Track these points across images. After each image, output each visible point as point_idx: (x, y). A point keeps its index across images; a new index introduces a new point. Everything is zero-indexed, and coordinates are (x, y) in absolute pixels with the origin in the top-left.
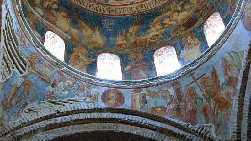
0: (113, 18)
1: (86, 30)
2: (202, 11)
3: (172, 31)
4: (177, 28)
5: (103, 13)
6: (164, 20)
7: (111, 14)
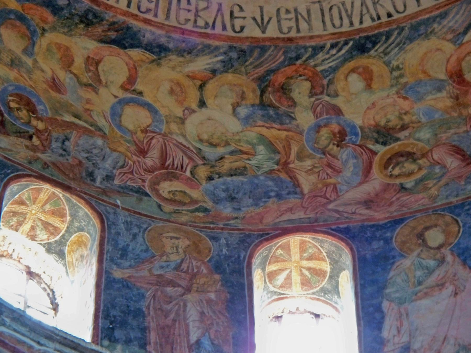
2: (41, 126)
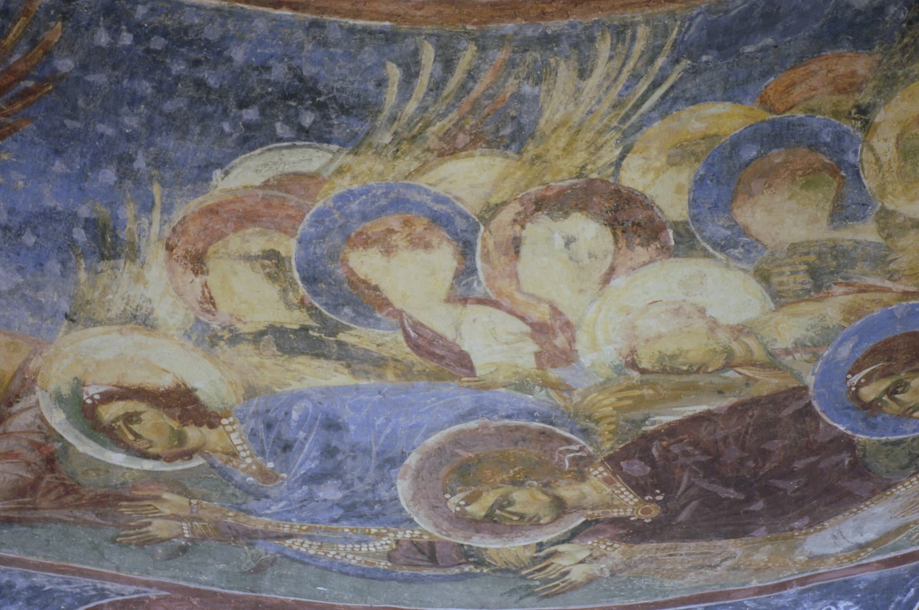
3: (440, 450)
4: (511, 454)
6: (366, 242)
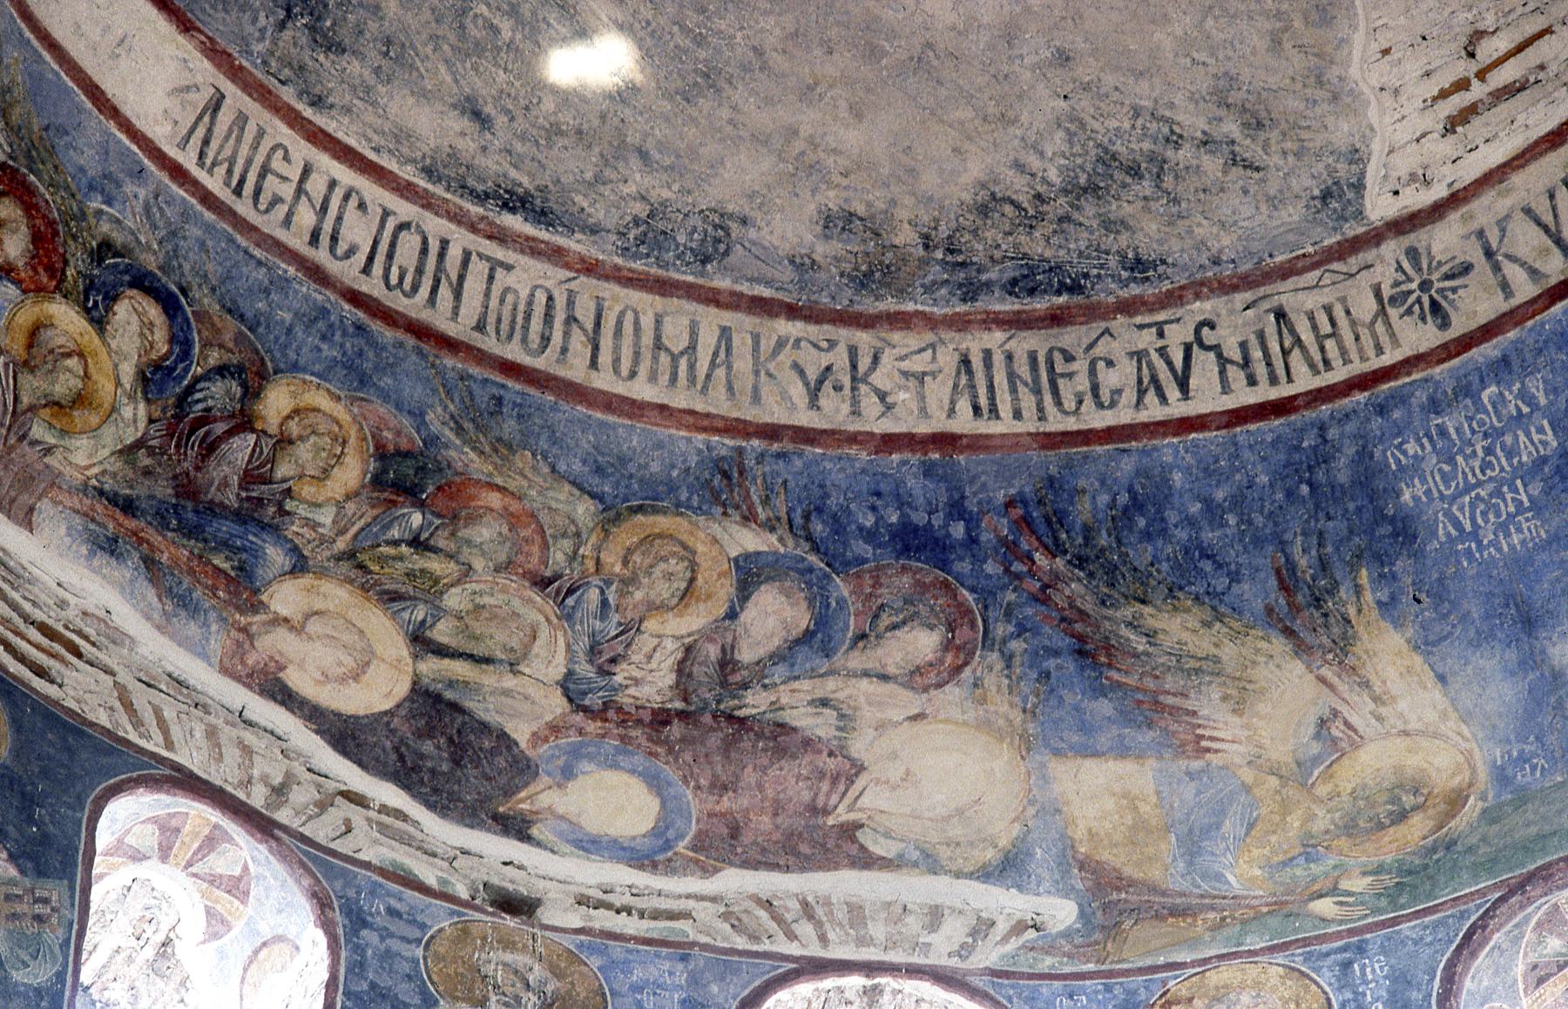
0: (1502, 367)
1: (1241, 697)
5: (1357, 368)
7: (1460, 325)
